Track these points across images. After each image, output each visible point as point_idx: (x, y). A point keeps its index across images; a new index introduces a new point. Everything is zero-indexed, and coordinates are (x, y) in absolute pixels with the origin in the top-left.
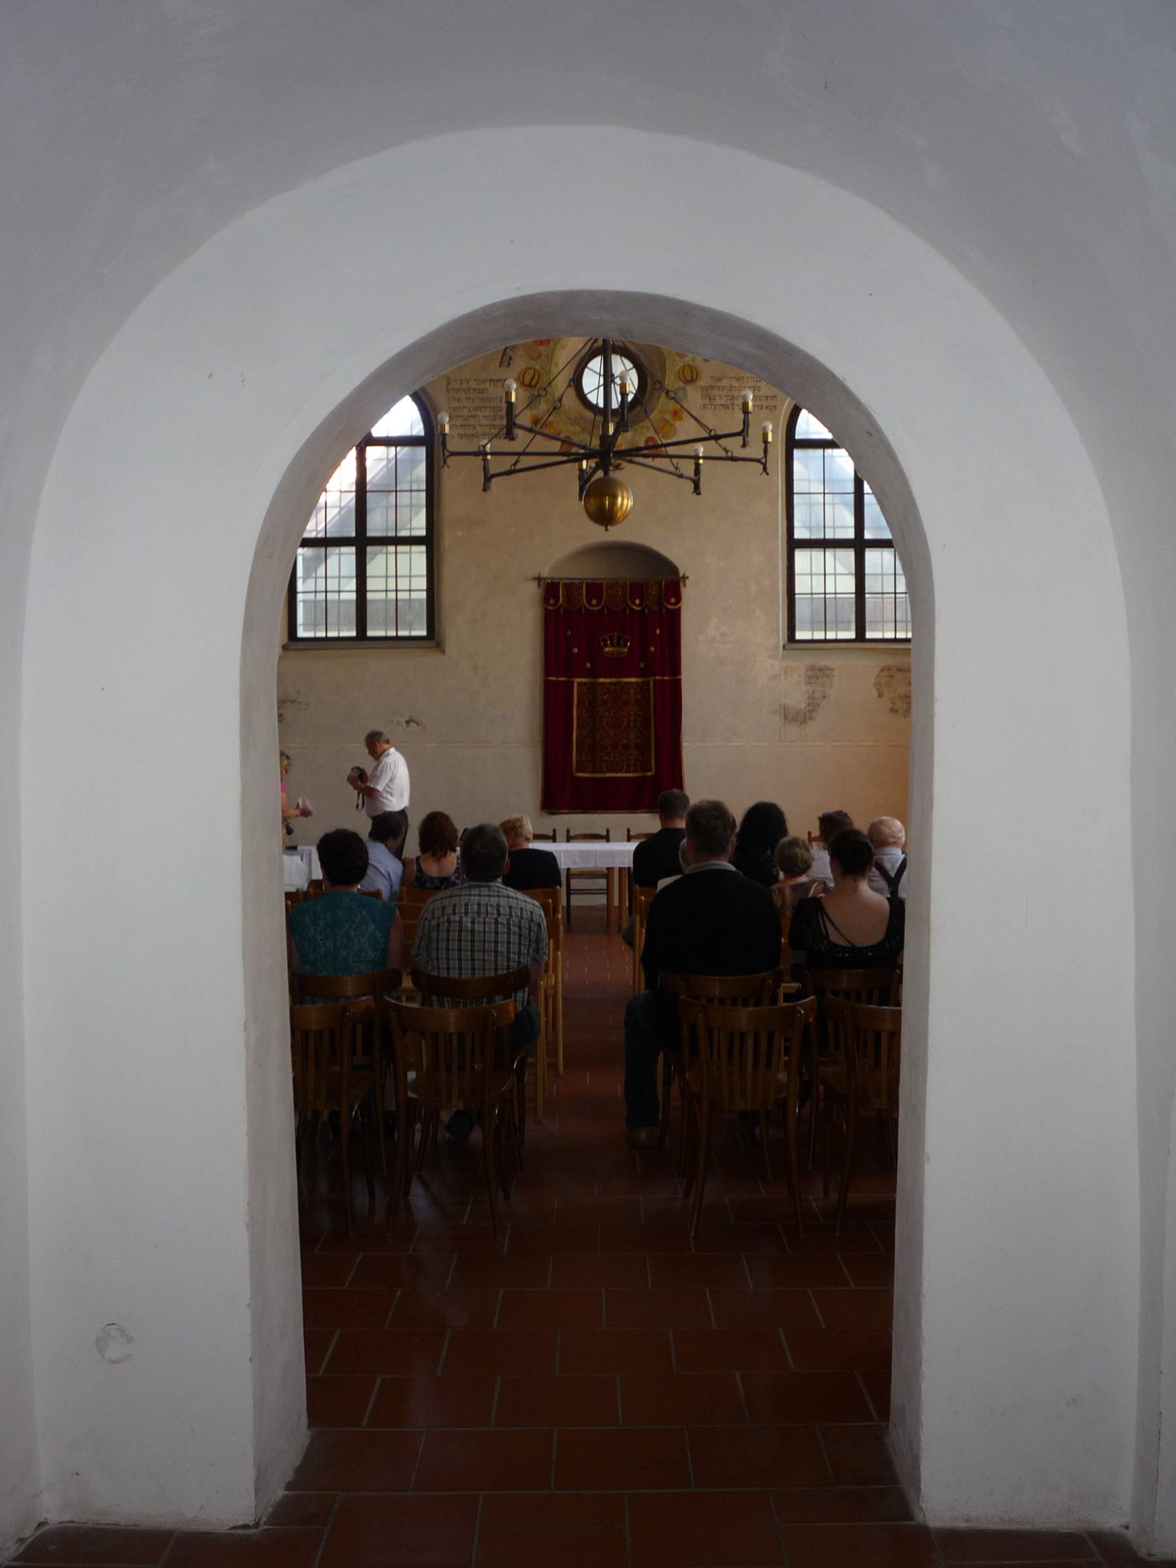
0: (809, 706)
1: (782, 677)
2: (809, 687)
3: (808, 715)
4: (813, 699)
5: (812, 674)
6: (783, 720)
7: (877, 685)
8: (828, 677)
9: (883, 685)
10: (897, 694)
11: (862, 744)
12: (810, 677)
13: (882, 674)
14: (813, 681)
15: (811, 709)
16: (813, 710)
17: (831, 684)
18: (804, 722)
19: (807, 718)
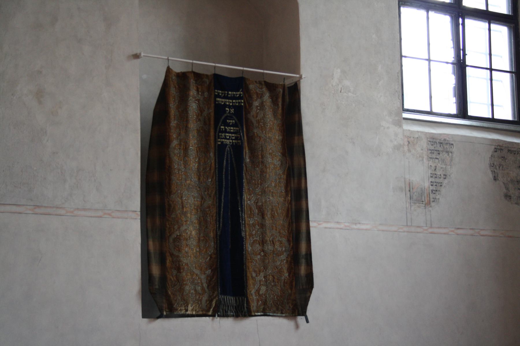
0: (432, 185)
1: (406, 148)
2: (431, 163)
3: (432, 196)
4: (436, 177)
5: (432, 148)
6: (409, 200)
7: (492, 165)
8: (447, 152)
9: (497, 167)
10: (509, 179)
11: (482, 233)
12: (432, 152)
13: (496, 154)
14: (434, 156)
15: (434, 189)
16: (436, 191)
17: (451, 160)
18: (429, 203)
19: (432, 200)
